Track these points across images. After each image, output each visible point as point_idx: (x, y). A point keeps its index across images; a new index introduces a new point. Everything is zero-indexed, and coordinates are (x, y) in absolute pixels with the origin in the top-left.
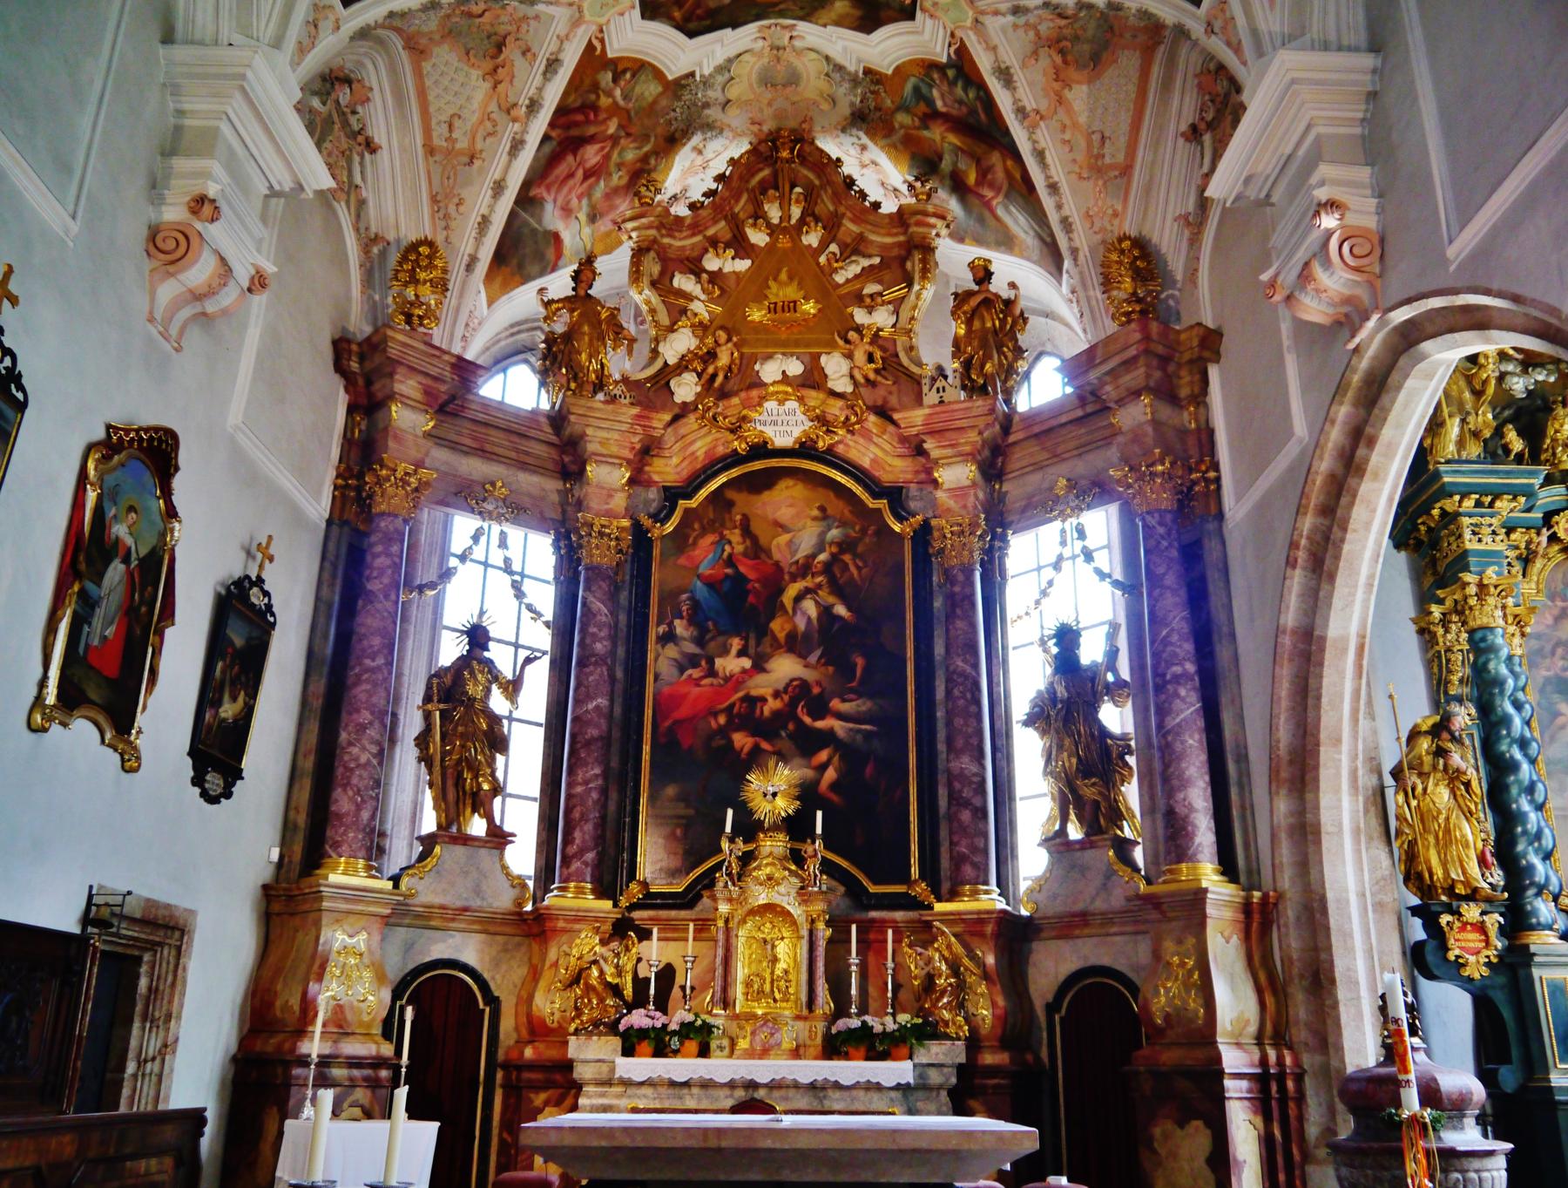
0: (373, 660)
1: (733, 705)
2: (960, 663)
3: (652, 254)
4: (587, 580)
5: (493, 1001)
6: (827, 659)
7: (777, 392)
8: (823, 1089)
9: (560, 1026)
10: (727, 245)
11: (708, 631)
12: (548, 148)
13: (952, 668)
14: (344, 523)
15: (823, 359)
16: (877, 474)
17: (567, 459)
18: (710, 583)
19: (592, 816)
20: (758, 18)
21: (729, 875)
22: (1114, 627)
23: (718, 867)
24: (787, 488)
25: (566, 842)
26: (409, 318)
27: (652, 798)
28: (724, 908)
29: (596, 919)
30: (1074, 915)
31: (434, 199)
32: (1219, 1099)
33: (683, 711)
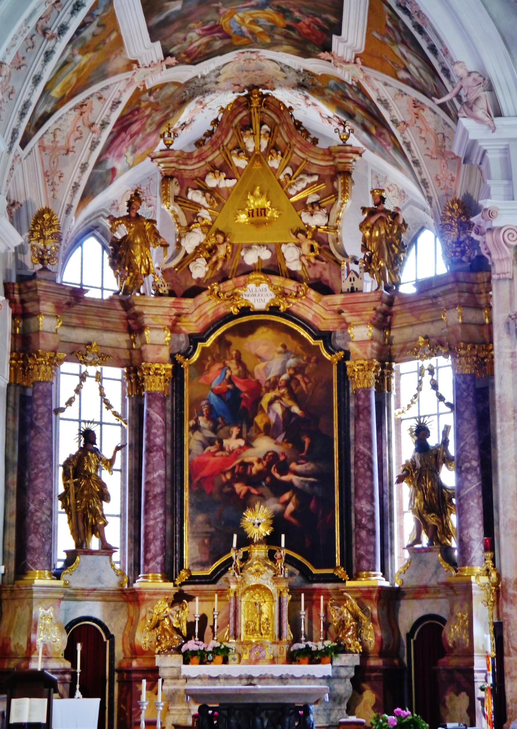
0: (44, 465)
1: (234, 468)
2: (361, 447)
3: (175, 180)
4: (149, 400)
5: (111, 637)
6: (288, 439)
7: (256, 279)
8: (286, 679)
9: (150, 650)
10: (221, 171)
11: (218, 423)
12: (111, 137)
13: (357, 450)
14: (17, 385)
15: (283, 247)
16: (316, 324)
17: (131, 322)
18: (219, 394)
19: (159, 537)
21: (236, 569)
22: (447, 429)
23: (231, 560)
24: (262, 333)
25: (146, 551)
26: (42, 261)
27: (192, 521)
28: (233, 587)
29: (165, 594)
30: (420, 587)
31: (46, 174)
32: (471, 682)
33: (206, 472)
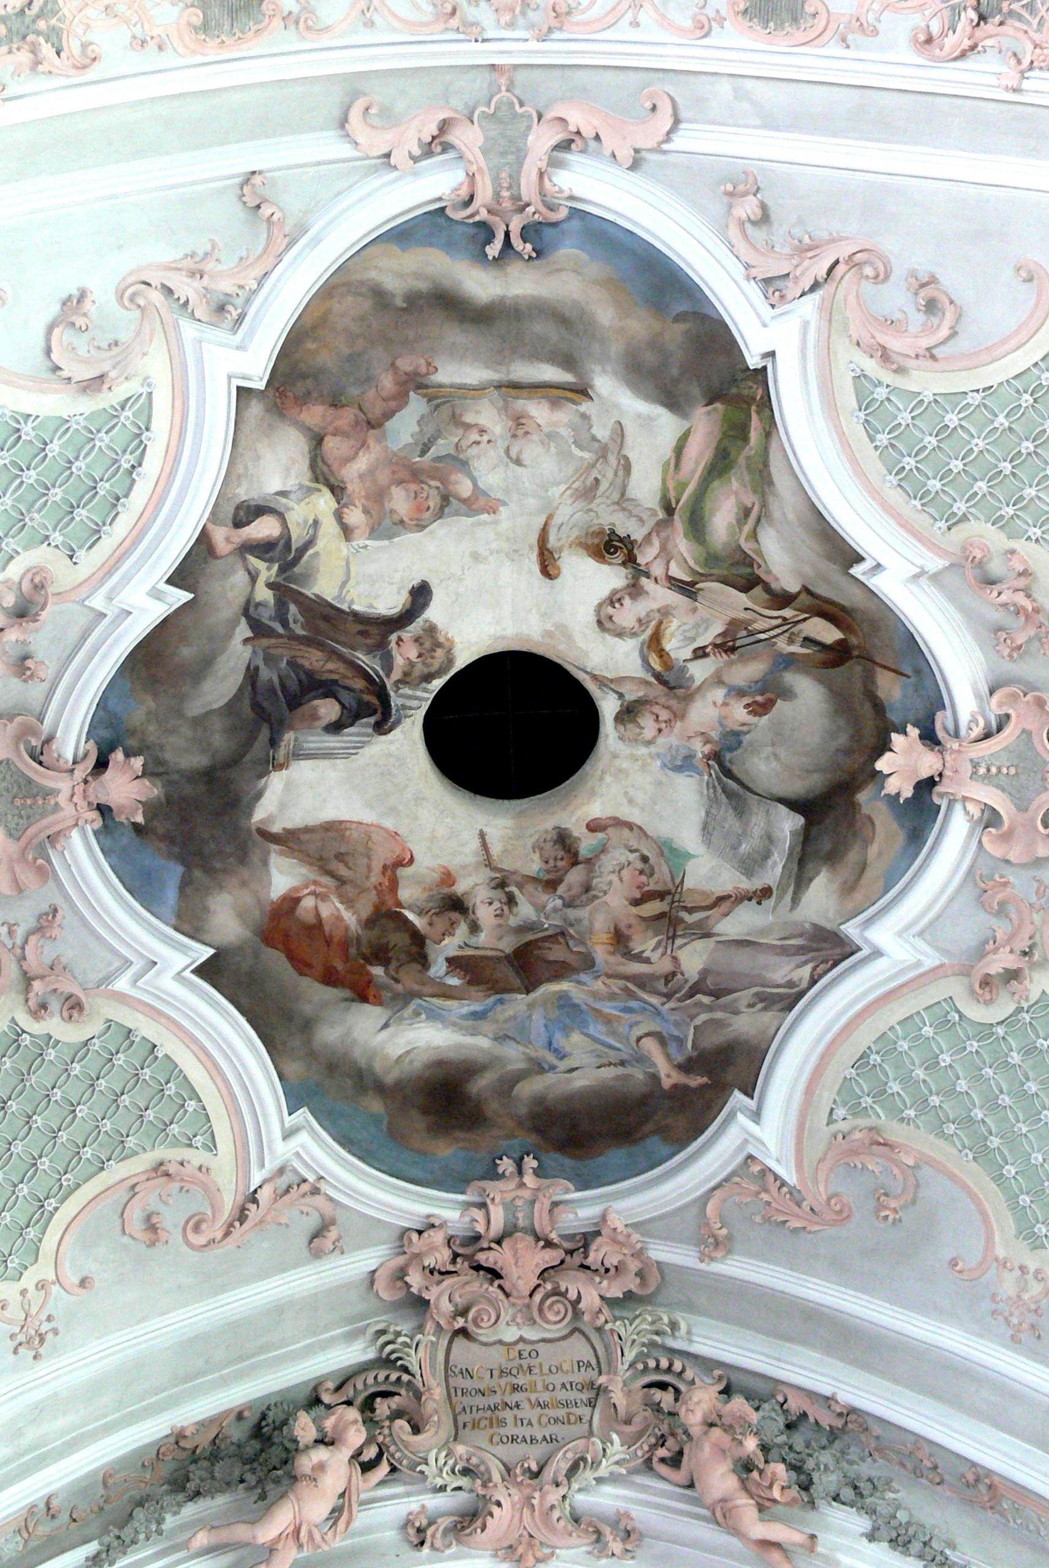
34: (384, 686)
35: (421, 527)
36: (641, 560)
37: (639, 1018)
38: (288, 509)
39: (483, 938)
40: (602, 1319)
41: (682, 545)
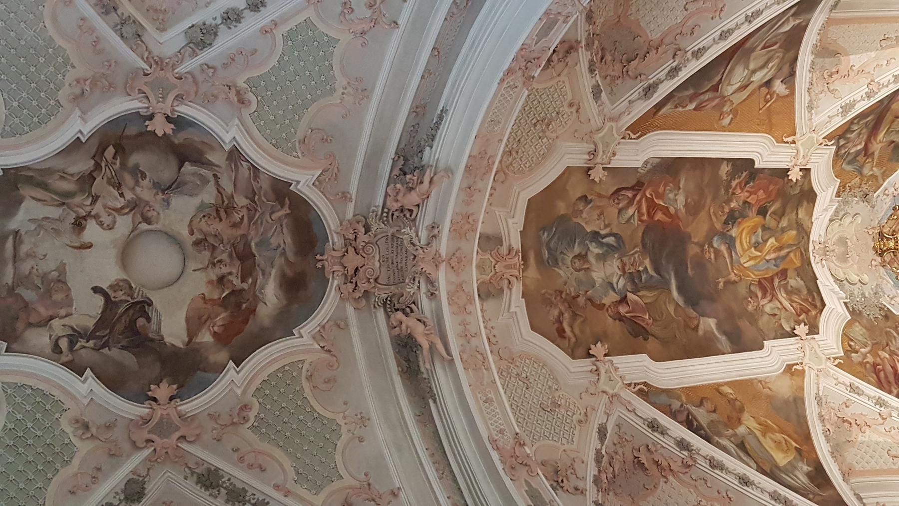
20: (810, 264)
34: (133, 303)
35: (69, 289)
36: (84, 214)
37: (264, 221)
38: (57, 335)
39: (234, 271)
40: (371, 235)
41: (77, 200)
